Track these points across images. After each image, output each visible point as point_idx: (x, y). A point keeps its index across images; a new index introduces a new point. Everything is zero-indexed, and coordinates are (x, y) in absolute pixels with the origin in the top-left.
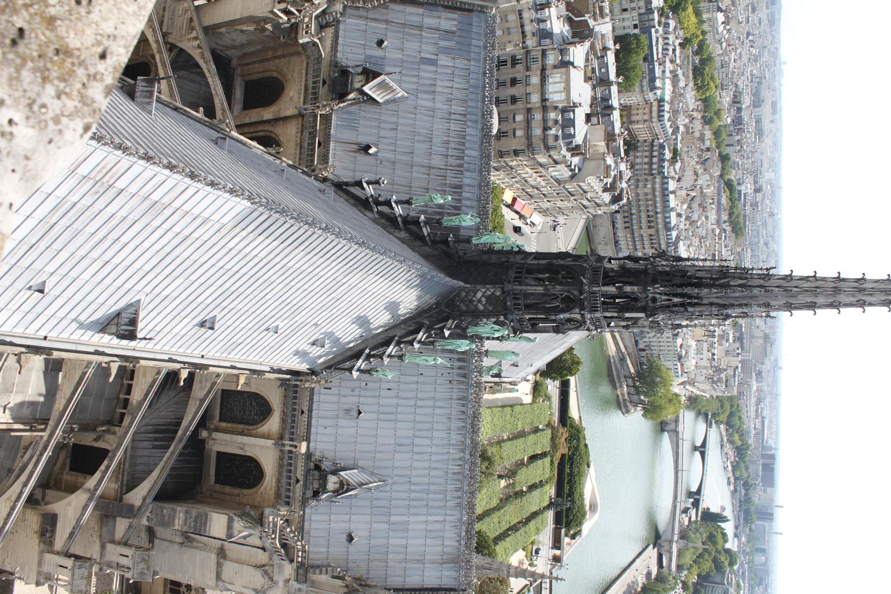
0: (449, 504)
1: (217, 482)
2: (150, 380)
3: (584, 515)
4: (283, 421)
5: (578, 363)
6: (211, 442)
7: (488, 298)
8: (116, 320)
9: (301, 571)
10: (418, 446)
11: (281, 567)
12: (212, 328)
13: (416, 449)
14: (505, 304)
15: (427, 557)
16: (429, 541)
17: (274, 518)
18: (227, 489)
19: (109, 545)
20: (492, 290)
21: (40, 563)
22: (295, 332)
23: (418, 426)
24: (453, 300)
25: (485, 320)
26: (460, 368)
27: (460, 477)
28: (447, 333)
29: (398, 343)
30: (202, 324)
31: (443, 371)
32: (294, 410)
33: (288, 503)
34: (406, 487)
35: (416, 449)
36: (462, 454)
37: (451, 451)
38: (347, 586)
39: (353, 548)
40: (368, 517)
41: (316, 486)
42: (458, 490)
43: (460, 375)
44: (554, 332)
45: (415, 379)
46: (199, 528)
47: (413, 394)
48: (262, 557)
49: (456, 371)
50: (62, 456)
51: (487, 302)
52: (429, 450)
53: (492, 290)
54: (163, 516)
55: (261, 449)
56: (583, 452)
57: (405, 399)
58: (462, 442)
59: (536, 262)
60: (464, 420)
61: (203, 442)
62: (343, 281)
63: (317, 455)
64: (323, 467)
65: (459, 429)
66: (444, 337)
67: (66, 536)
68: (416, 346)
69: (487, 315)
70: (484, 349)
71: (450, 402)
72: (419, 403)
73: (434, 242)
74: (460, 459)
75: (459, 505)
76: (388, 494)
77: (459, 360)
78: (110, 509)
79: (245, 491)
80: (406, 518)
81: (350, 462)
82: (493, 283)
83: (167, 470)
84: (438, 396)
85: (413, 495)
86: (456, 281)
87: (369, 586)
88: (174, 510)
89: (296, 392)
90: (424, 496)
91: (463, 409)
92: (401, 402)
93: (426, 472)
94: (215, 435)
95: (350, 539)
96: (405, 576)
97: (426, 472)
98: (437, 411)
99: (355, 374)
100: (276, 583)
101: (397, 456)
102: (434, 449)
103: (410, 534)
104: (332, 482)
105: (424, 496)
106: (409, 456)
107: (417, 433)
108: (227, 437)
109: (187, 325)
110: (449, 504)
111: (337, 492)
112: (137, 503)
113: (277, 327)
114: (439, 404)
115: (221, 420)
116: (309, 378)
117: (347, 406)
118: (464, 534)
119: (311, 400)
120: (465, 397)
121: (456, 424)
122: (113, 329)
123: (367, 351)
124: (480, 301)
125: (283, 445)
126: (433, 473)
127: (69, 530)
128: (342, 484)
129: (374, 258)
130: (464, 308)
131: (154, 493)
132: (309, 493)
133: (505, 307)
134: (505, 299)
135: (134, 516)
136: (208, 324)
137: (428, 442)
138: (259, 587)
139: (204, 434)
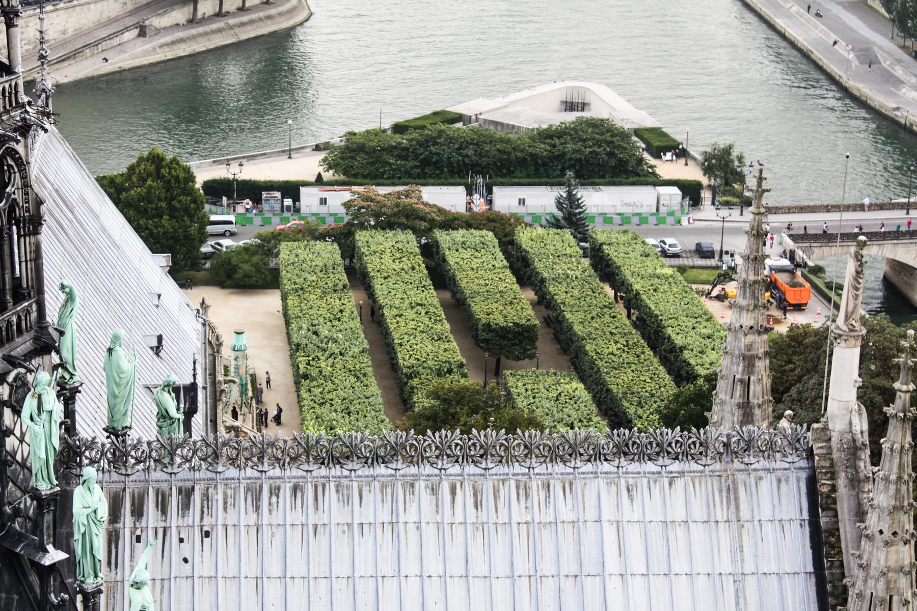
0: (566, 512)
3: (598, 125)
15: (726, 566)
16: (681, 565)
25: (11, 442)
26: (163, 506)
28: (54, 556)
31: (176, 559)
36: (421, 485)
37: (412, 516)
42: (524, 490)
43: (186, 506)
44: (36, 232)
52: (414, 582)
56: (415, 135)
58: (384, 487)
60: (319, 489)
65: (347, 500)
66: (72, 564)
70: (102, 438)
71: (266, 531)
74: (434, 490)
77: (138, 512)
84: (249, 568)
93: (478, 587)
98: (296, 567)
105: (550, 583)
118: (650, 467)
120: (248, 489)
121: (333, 509)
126: (479, 567)
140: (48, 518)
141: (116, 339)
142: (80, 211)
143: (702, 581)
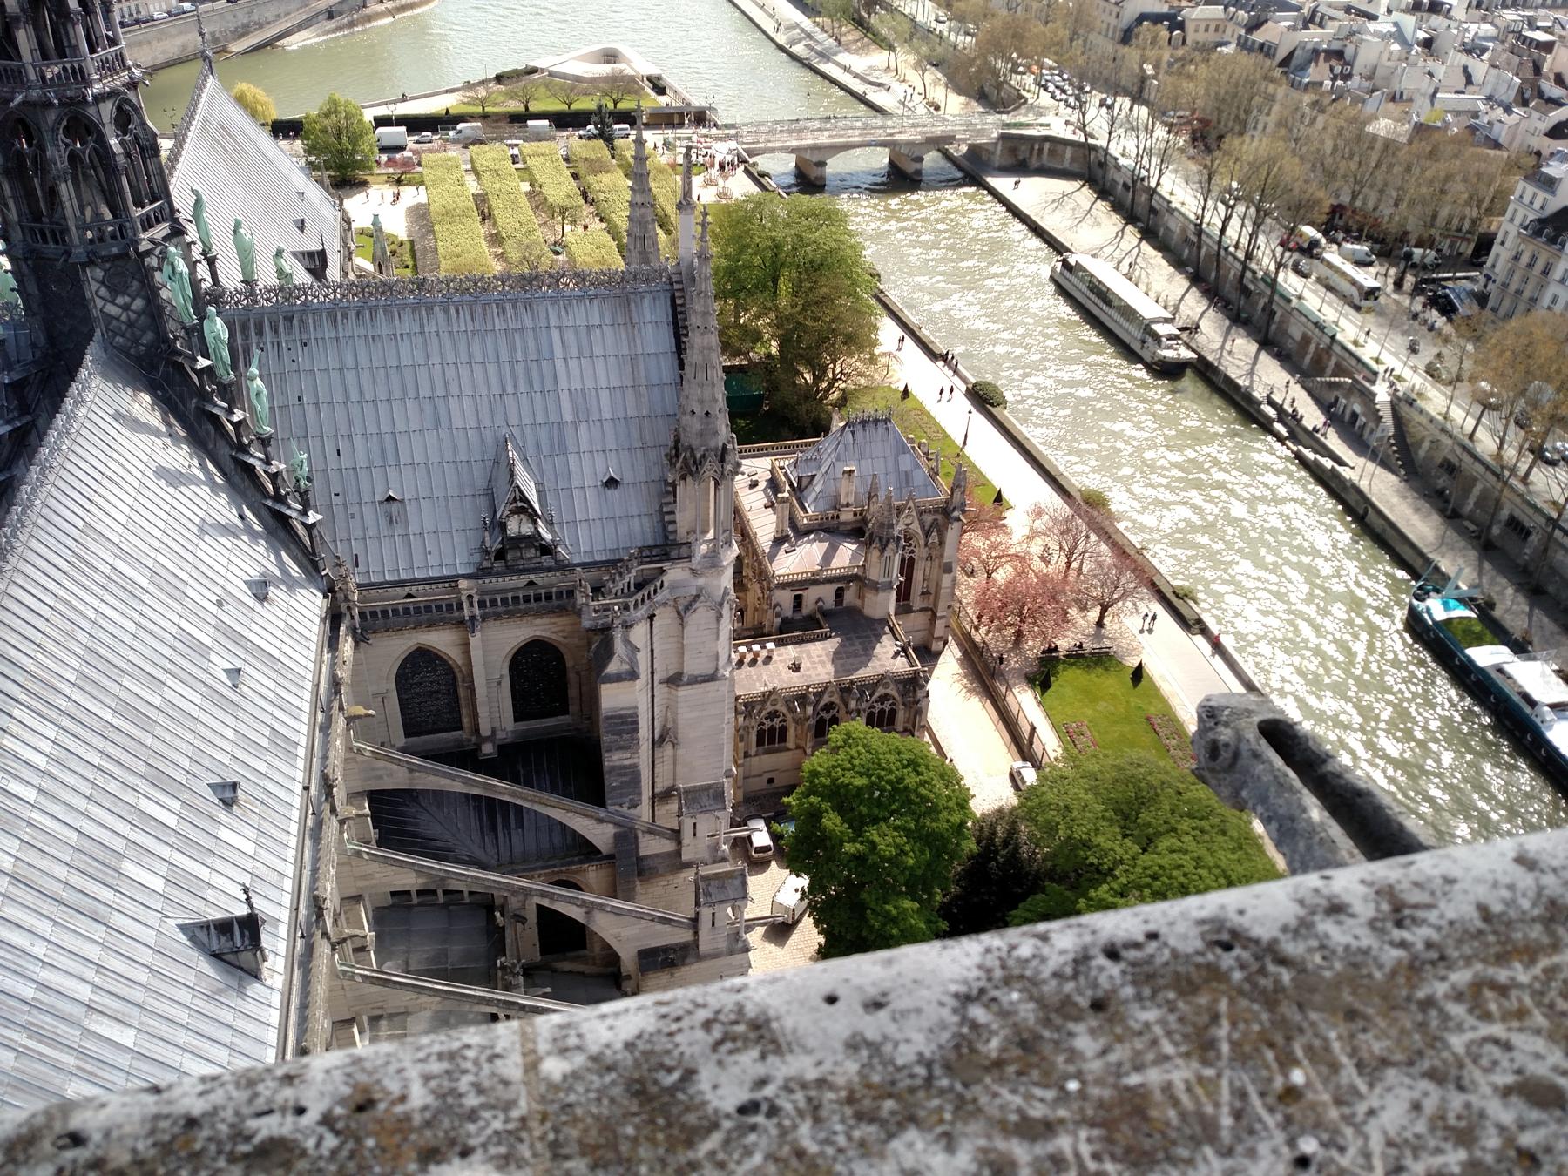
0: (529, 324)
1: (566, 712)
2: (374, 866)
4: (431, 625)
5: (334, 102)
6: (500, 735)
7: (115, 291)
8: (230, 957)
9: (674, 554)
10: (433, 389)
11: (673, 587)
12: (234, 786)
13: (440, 392)
14: (117, 257)
16: (598, 351)
17: (590, 611)
18: (573, 692)
19: (685, 857)
20: (94, 286)
21: (715, 956)
22: (237, 638)
23: (397, 394)
24: (138, 360)
25: (164, 294)
26: (275, 330)
27: (479, 310)
28: (203, 363)
29: (244, 449)
30: (228, 804)
32: (407, 611)
33: (571, 593)
34: (510, 401)
35: (440, 392)
38: (684, 478)
39: (628, 477)
40: (572, 459)
41: (532, 552)
43: (290, 328)
45: (310, 411)
46: (627, 723)
47: (340, 411)
48: (665, 618)
49: (283, 338)
50: (566, 966)
51: (124, 293)
52: (437, 370)
53: (94, 286)
54: (624, 785)
55: (489, 652)
57: (350, 422)
59: (11, 202)
60: (373, 312)
61: (502, 748)
62: (107, 570)
63: (477, 558)
64: (497, 546)
67: (667, 928)
68: (238, 415)
69: (150, 292)
70: (241, 286)
72: (354, 396)
73: (24, 409)
74: (446, 311)
75: (528, 305)
76: (528, 431)
77: (260, 333)
78: (627, 868)
79: (569, 664)
80: (565, 396)
81: (483, 502)
82: (77, 284)
83: (546, 796)
85: (522, 388)
86: (88, 358)
87: (677, 441)
88: (613, 768)
89: (374, 614)
90: (521, 366)
91: (352, 314)
92: (357, 429)
93: (478, 369)
94: (485, 731)
95: (612, 483)
96: (661, 385)
97: (478, 369)
99: (313, 517)
100: (700, 589)
101: (458, 422)
102: (435, 360)
103: (589, 384)
104: (516, 526)
106: (453, 403)
107: (411, 393)
108: (483, 711)
109: (234, 834)
110: (529, 324)
111: (533, 517)
112: (610, 830)
113: (227, 671)
114: (350, 363)
115: (461, 728)
116: (340, 596)
117: (383, 522)
119: (384, 585)
122: (245, 958)
123: (269, 503)
124: (126, 307)
125: (473, 618)
126: (478, 358)
127: (659, 927)
128: (513, 512)
129: (41, 522)
130: (148, 337)
131: (589, 808)
132: (547, 561)
133: (124, 255)
134: (105, 259)
135: (632, 830)
136: (228, 795)
137: (423, 374)
138: (713, 614)
139: (488, 748)
140: (195, 340)
141: (238, 225)
142: (240, 138)
143: (612, 360)
